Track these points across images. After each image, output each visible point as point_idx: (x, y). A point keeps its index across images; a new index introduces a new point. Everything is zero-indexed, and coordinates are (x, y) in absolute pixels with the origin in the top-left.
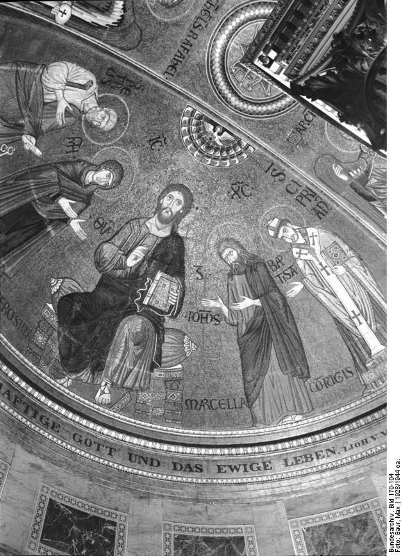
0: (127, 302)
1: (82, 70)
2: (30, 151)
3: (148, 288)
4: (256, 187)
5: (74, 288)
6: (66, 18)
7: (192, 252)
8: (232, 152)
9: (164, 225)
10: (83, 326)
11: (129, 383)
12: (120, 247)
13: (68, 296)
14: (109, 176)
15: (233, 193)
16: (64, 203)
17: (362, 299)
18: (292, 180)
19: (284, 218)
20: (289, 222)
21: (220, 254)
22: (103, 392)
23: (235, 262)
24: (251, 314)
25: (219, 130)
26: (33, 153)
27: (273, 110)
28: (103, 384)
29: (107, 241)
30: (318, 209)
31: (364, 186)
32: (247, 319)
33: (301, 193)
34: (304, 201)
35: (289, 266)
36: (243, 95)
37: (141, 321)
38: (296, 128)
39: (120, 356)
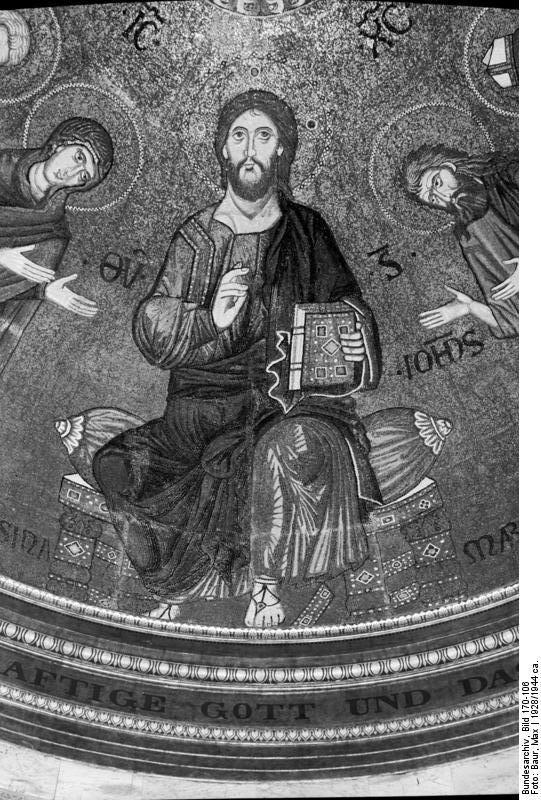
3: (288, 352)
5: (121, 425)
7: (349, 226)
10: (170, 490)
11: (318, 565)
12: (184, 298)
13: (112, 443)
14: (81, 158)
15: (370, 43)
21: (413, 197)
22: (262, 605)
23: (455, 195)
28: (258, 588)
29: (149, 297)
37: (300, 428)
39: (278, 520)
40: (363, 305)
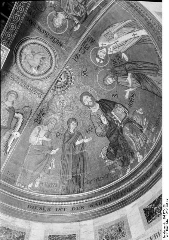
0: (118, 130)
1: (34, 131)
2: (56, 152)
3: (116, 119)
4: (83, 66)
6: (18, 134)
7: (107, 96)
8: (69, 74)
9: (95, 105)
10: (118, 151)
11: (142, 145)
13: (107, 152)
14: (73, 124)
15: (85, 75)
16: (78, 143)
17: (127, 30)
18: (79, 51)
19: (95, 56)
20: (97, 53)
21: (109, 85)
22: (139, 157)
24: (133, 79)
25: (60, 79)
26: (58, 151)
27: (54, 55)
28: (137, 155)
29: (95, 129)
30: (90, 41)
31: (81, 18)
32: (135, 82)
33: (85, 48)
34: (88, 46)
35: (115, 57)
36: (49, 67)
37: (126, 127)
38: (61, 46)
39: (133, 142)
40: (118, 104)
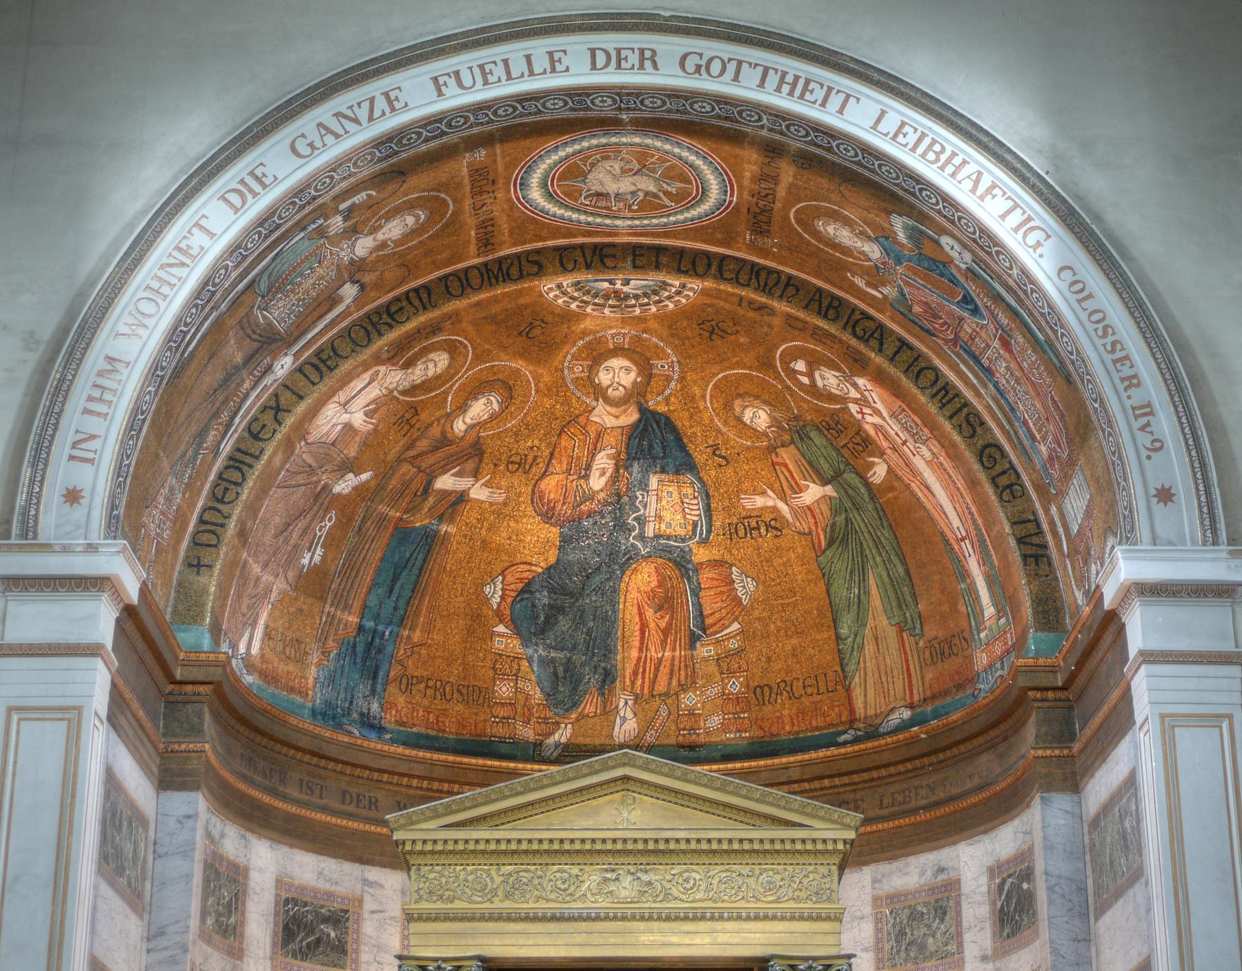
2: (356, 489)
5: (526, 575)
10: (564, 623)
11: (661, 687)
12: (568, 472)
13: (522, 591)
16: (446, 482)
22: (624, 719)
23: (769, 427)
28: (622, 704)
40: (700, 480)
